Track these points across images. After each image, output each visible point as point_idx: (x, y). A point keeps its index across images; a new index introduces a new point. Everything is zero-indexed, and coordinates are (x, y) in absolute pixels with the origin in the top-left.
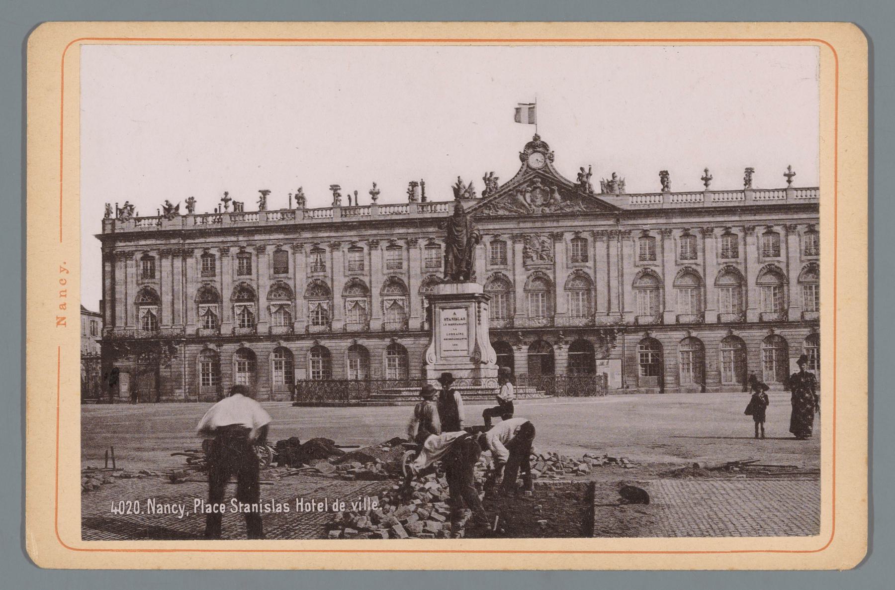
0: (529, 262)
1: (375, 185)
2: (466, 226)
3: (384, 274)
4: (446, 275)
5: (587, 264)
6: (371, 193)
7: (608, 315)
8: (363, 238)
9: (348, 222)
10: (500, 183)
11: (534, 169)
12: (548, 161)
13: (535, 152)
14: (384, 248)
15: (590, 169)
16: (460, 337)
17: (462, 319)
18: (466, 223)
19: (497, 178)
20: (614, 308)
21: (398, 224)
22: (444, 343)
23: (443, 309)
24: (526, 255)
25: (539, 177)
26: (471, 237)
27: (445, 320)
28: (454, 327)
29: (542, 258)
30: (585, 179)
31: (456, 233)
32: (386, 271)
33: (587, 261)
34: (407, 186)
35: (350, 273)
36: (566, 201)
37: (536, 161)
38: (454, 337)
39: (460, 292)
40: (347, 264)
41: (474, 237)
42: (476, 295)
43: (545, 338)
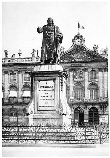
0: (75, 79)
1: (20, 51)
2: (54, 30)
3: (23, 83)
4: (41, 61)
5: (96, 80)
6: (19, 54)
7: (104, 98)
8: (16, 70)
9: (10, 64)
10: (65, 50)
11: (78, 45)
12: (83, 42)
13: (78, 39)
14: (23, 73)
15: (98, 45)
16: (50, 98)
17: (51, 87)
18: (54, 29)
19: (64, 49)
20: (106, 97)
21: (28, 65)
22: (39, 101)
23: (39, 80)
24: (74, 77)
25: (79, 48)
26: (57, 37)
27: (40, 87)
28: (46, 92)
29: (80, 78)
30: (96, 49)
31: (48, 35)
32: (24, 82)
33: (96, 79)
34: (31, 51)
35: (11, 82)
36: (89, 57)
37: (78, 42)
38: (46, 98)
39: (50, 70)
40: (10, 79)
41: (59, 37)
42: (60, 72)
43: (80, 107)
